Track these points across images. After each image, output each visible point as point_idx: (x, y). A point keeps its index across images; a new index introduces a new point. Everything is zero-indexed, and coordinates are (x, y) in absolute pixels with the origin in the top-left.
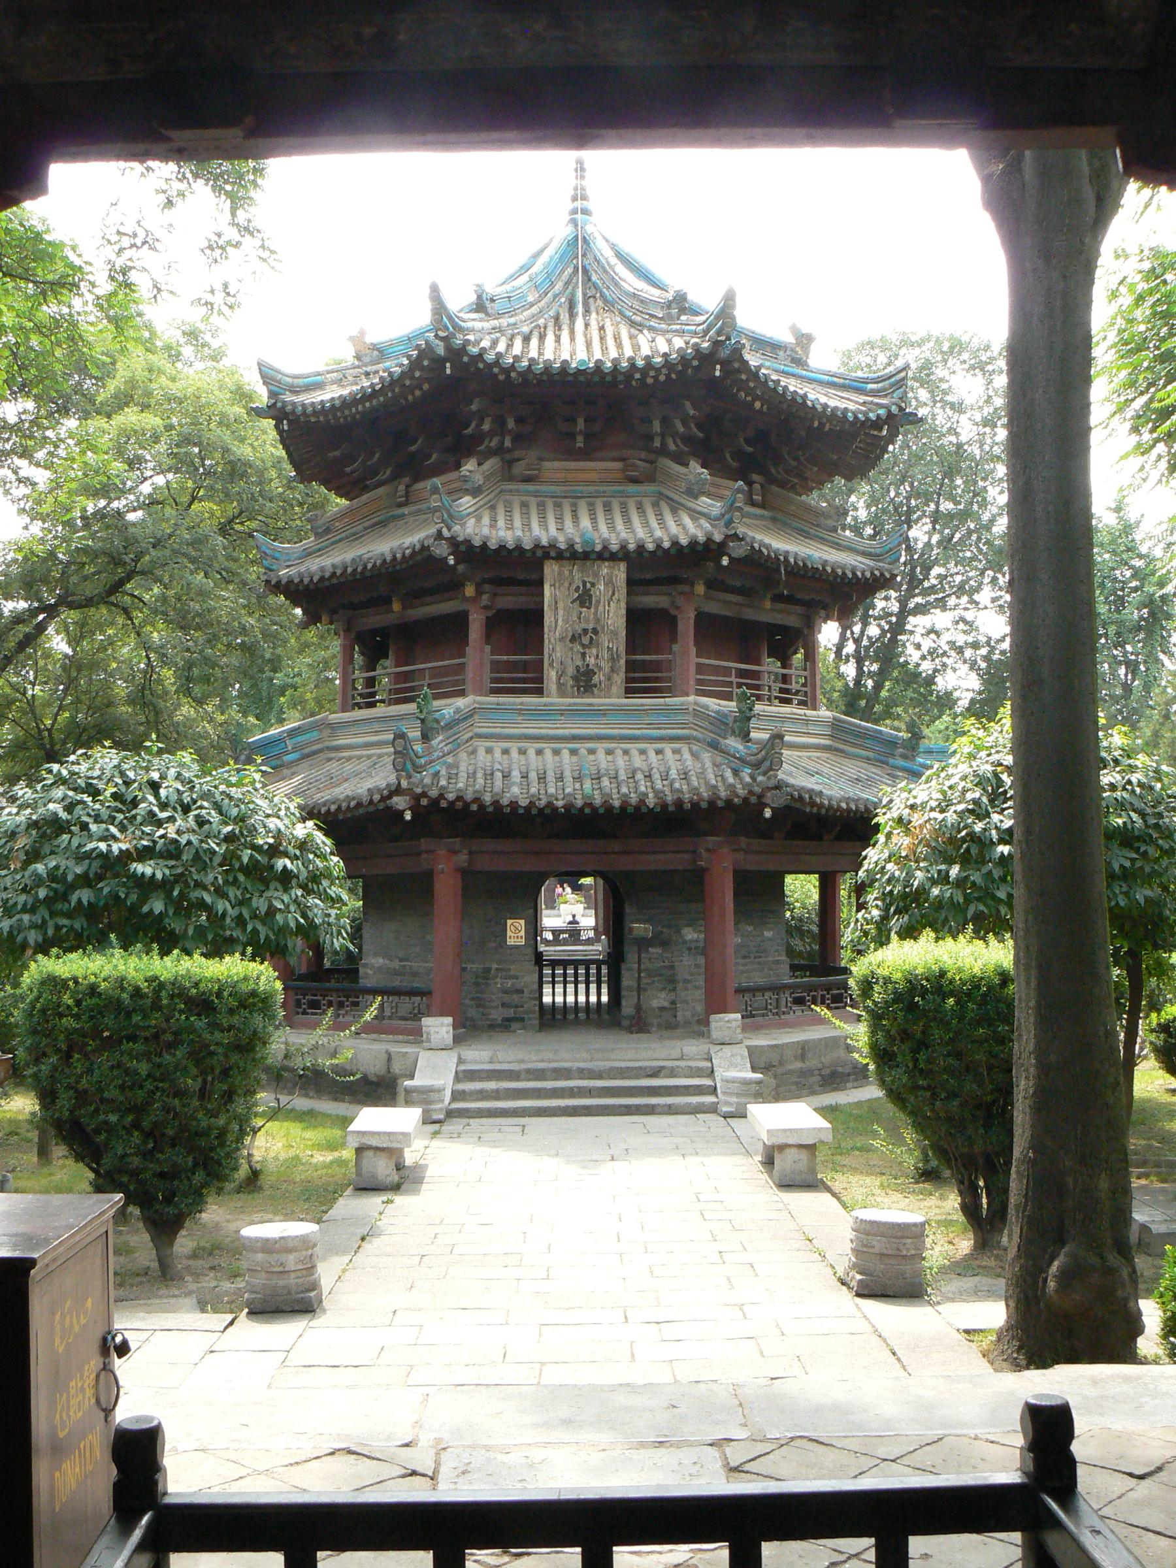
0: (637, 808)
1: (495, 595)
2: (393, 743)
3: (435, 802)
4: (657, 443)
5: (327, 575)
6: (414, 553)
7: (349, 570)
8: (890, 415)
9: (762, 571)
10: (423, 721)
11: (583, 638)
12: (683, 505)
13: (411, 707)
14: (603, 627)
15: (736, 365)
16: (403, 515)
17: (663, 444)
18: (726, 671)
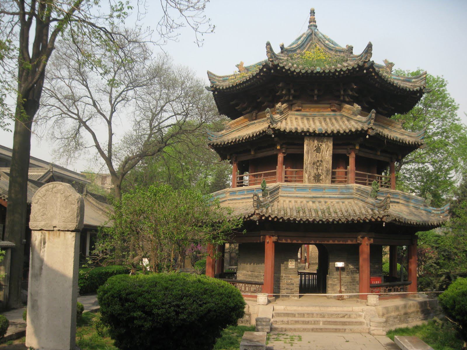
0: (338, 222)
1: (287, 149)
2: (253, 198)
3: (267, 218)
4: (342, 98)
5: (230, 142)
6: (260, 133)
7: (237, 140)
8: (421, 89)
9: (379, 141)
10: (263, 190)
11: (317, 164)
12: (350, 118)
13: (259, 186)
14: (324, 160)
15: (371, 70)
16: (255, 123)
17: (344, 98)
18: (365, 176)
